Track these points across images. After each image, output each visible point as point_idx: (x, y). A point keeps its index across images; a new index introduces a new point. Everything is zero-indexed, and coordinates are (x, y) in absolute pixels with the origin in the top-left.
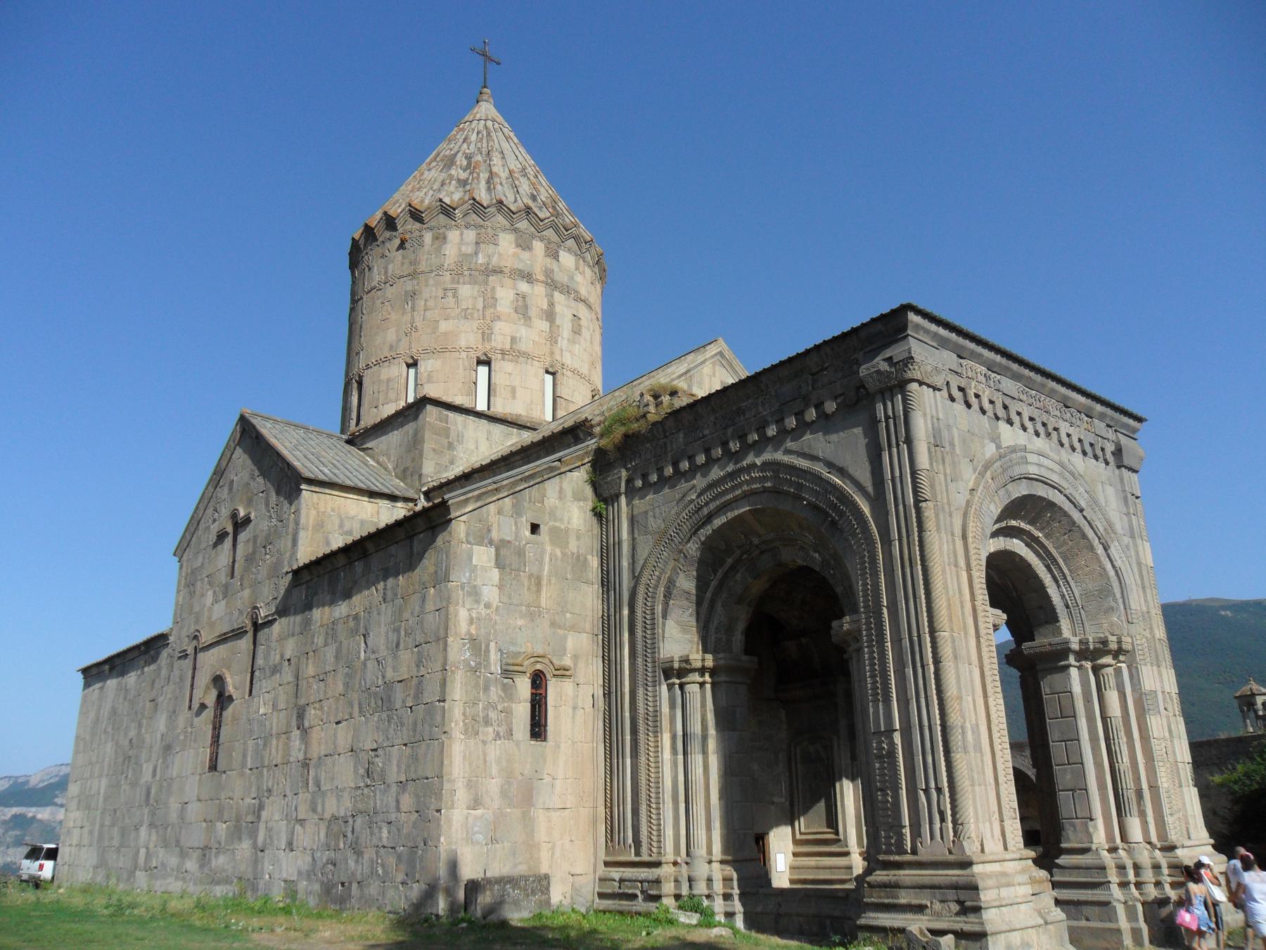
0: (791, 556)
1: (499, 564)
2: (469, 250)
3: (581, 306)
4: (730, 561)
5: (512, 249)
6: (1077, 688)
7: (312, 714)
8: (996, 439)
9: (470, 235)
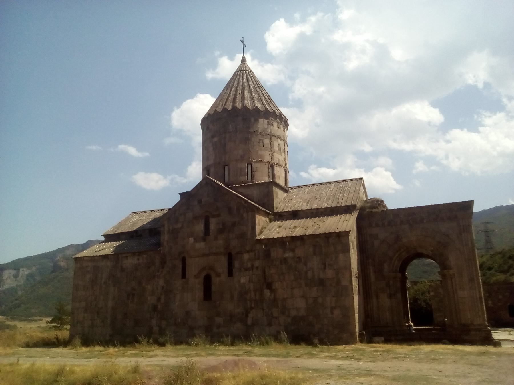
2: (266, 126)
4: (402, 250)
5: (277, 128)
7: (277, 285)
9: (266, 122)
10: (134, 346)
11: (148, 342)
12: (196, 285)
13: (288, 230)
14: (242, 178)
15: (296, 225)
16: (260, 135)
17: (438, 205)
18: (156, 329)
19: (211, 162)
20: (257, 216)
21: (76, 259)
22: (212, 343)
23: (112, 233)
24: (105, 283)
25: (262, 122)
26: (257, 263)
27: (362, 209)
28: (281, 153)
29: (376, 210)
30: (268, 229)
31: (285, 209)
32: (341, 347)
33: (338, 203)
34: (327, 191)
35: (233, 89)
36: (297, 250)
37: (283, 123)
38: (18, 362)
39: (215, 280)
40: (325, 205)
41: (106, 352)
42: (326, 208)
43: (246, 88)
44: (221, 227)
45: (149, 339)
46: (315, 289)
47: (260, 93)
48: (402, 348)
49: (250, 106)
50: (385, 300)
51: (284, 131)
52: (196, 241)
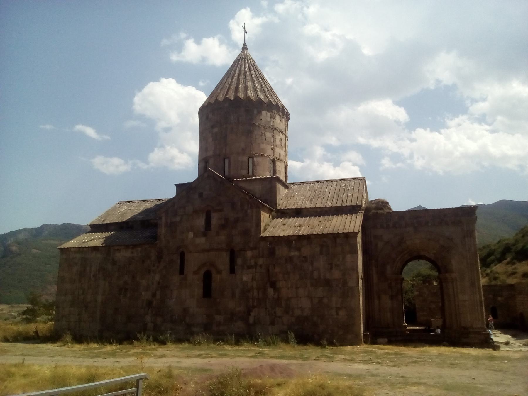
2: (269, 119)
4: (405, 252)
7: (281, 284)
9: (269, 114)
10: (131, 343)
11: (147, 340)
12: (195, 281)
13: (293, 228)
14: (244, 172)
15: (301, 223)
16: (263, 128)
17: (443, 209)
18: (150, 325)
19: (210, 153)
20: (262, 212)
21: (62, 250)
22: (216, 341)
23: (100, 223)
24: (94, 276)
25: (265, 115)
26: (261, 261)
27: (367, 210)
30: (273, 227)
31: (288, 206)
32: (349, 349)
33: (343, 202)
34: (331, 189)
35: (235, 78)
37: (285, 116)
38: (23, 362)
39: (216, 277)
40: (329, 204)
41: (103, 350)
42: (331, 207)
43: (249, 78)
44: (223, 222)
45: (149, 337)
46: (321, 288)
47: (263, 83)
48: (409, 350)
49: (252, 96)
50: (387, 302)
51: (285, 125)
52: (196, 235)
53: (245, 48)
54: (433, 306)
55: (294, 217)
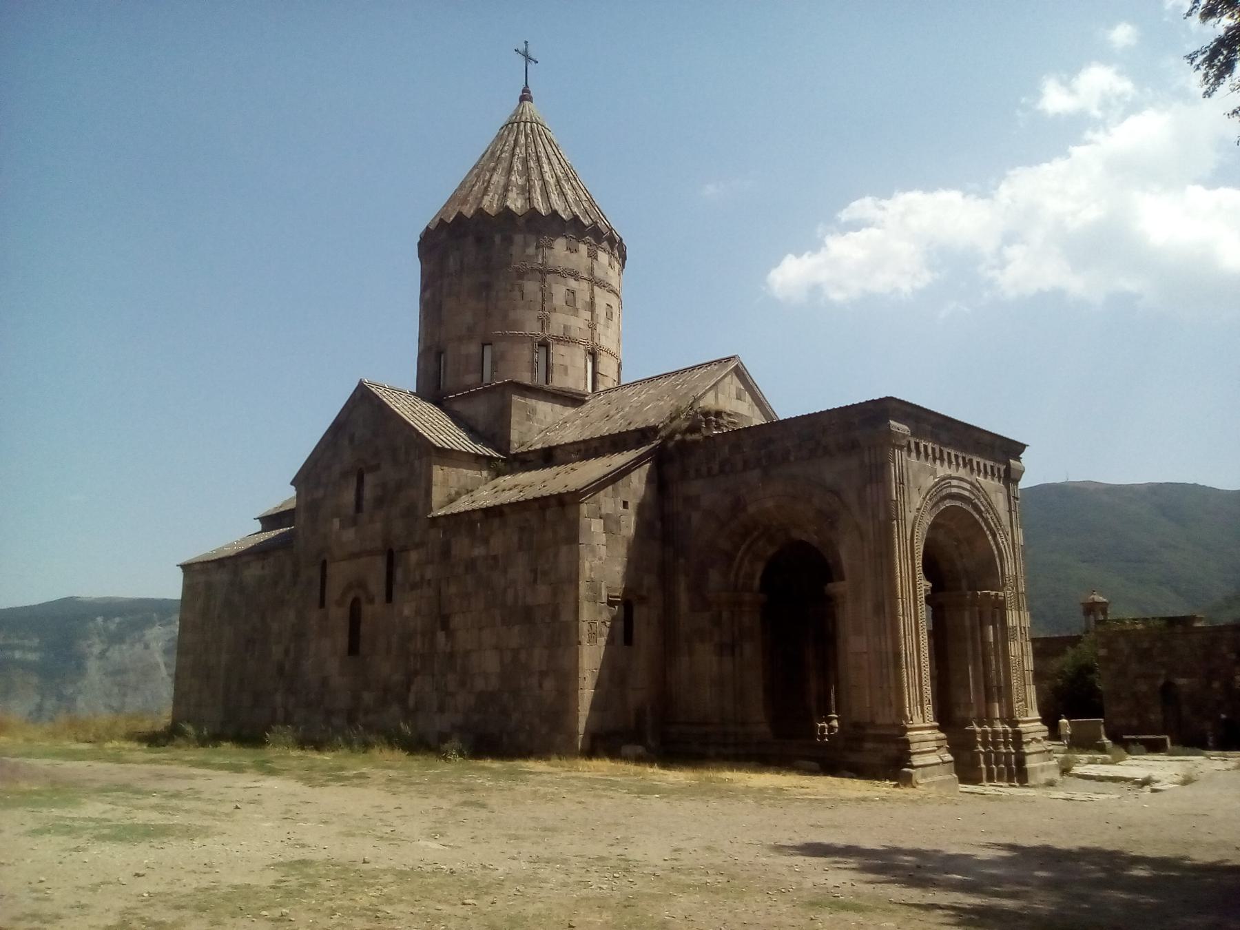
0: (796, 534)
1: (607, 530)
3: (612, 296)
4: (756, 534)
6: (967, 623)
7: (456, 621)
8: (934, 473)
14: (471, 379)
28: (575, 312)
29: (696, 436)
36: (492, 541)
39: (367, 610)
46: (516, 629)
52: (342, 527)
53: (525, 97)
54: (1143, 687)
55: (544, 468)
